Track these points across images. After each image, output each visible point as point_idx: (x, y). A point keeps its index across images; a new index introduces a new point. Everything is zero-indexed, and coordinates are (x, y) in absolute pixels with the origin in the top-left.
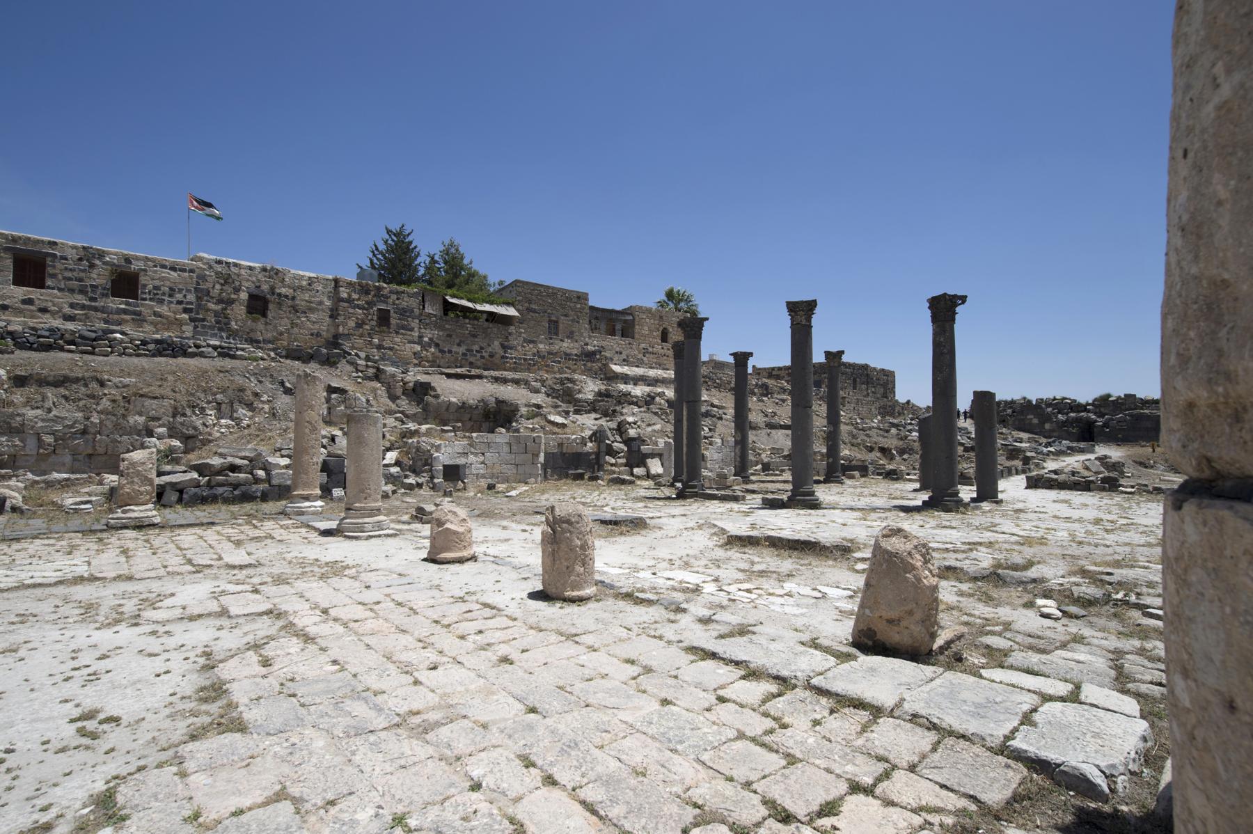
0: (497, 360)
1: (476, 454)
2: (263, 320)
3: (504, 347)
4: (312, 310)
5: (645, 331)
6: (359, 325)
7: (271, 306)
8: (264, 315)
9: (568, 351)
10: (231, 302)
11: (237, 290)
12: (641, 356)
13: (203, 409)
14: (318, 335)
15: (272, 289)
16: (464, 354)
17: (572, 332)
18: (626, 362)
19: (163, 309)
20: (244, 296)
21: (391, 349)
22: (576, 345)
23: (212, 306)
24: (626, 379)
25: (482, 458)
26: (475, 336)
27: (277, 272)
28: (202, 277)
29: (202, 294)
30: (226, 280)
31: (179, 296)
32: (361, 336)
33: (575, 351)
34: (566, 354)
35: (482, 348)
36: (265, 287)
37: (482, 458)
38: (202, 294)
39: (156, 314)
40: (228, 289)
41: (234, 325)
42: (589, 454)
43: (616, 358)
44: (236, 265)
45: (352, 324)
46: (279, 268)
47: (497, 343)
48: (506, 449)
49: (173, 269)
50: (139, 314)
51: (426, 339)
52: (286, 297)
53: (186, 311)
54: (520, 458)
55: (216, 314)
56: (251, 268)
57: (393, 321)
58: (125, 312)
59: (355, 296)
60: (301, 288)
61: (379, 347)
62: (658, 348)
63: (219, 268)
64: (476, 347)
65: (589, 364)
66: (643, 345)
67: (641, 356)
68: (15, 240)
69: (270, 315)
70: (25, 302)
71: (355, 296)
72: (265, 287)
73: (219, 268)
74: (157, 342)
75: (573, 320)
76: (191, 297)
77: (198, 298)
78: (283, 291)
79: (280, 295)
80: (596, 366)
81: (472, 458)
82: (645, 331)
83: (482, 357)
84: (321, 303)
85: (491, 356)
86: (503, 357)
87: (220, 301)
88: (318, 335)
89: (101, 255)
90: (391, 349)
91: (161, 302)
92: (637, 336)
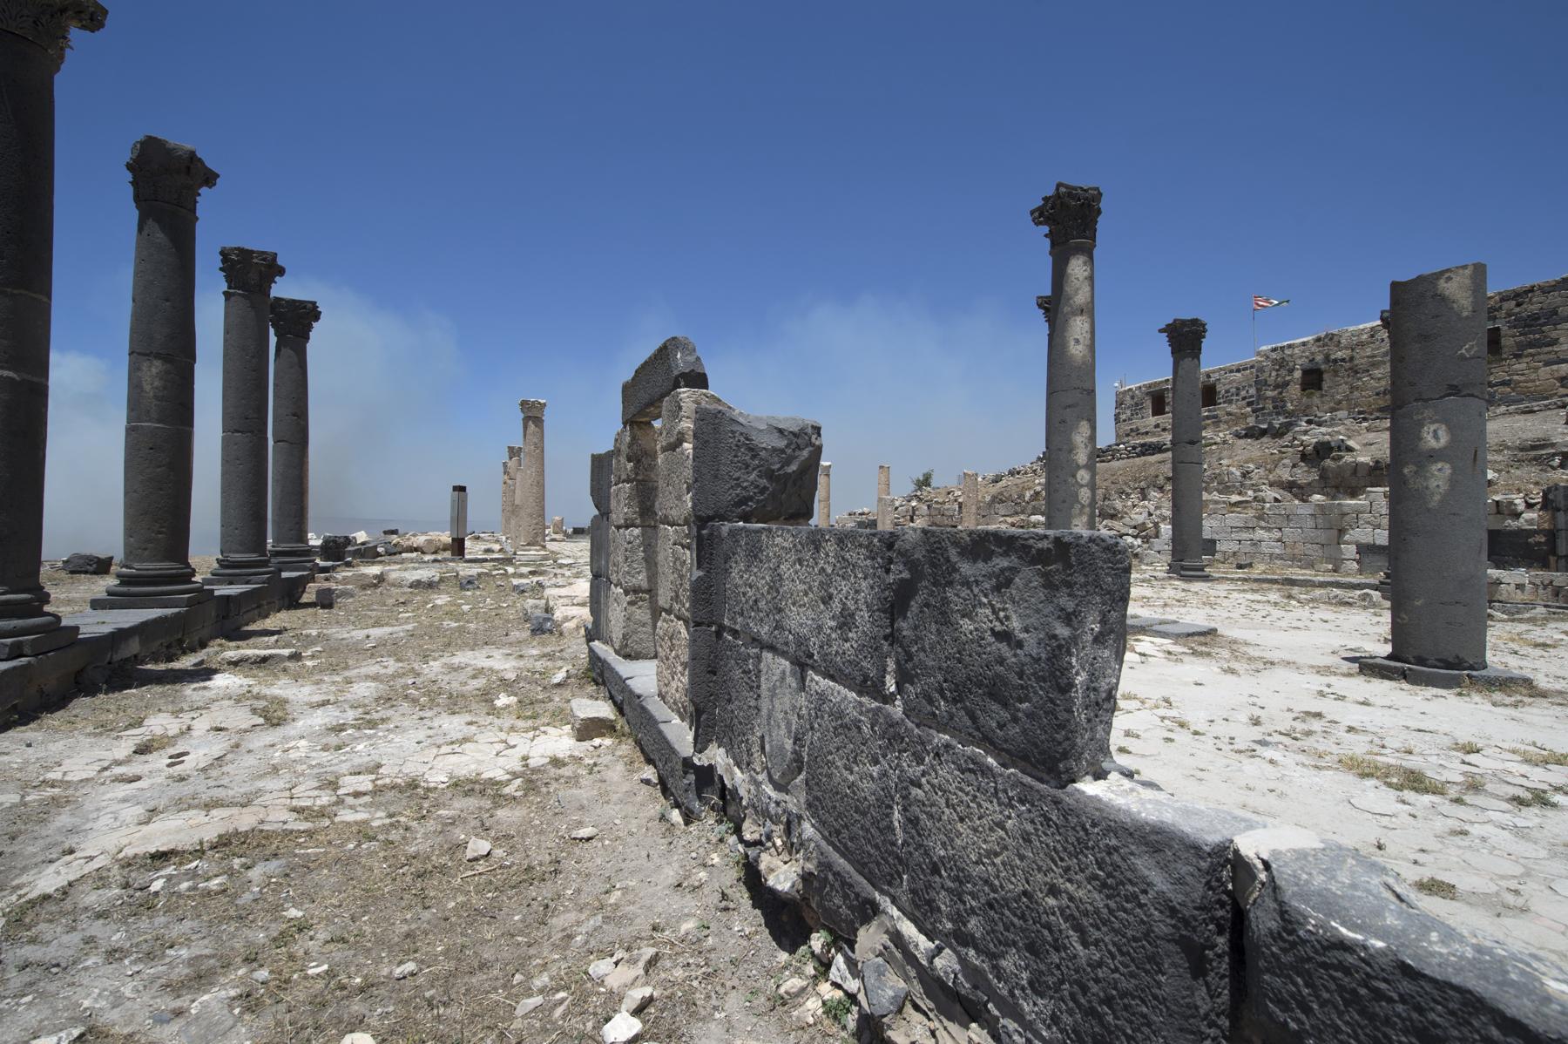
1: (1269, 529)
2: (1318, 393)
7: (1325, 376)
8: (1320, 388)
10: (1287, 384)
11: (1291, 371)
13: (1128, 495)
15: (1327, 357)
19: (1233, 408)
20: (1298, 374)
21: (1503, 383)
27: (1331, 337)
28: (1261, 370)
31: (1243, 393)
36: (1319, 358)
39: (1229, 414)
40: (1283, 372)
41: (1290, 406)
42: (1520, 532)
44: (1290, 346)
46: (1335, 331)
48: (1310, 523)
49: (1238, 371)
50: (1215, 417)
52: (1343, 360)
53: (1249, 404)
54: (1322, 536)
55: (1274, 399)
56: (1304, 344)
60: (1362, 344)
63: (1274, 356)
68: (1150, 386)
69: (1325, 386)
70: (1157, 426)
72: (1319, 358)
73: (1274, 356)
74: (1142, 445)
76: (1252, 391)
77: (1258, 390)
78: (1339, 354)
79: (1335, 361)
81: (1260, 534)
87: (1277, 387)
90: (1503, 383)
91: (1230, 402)
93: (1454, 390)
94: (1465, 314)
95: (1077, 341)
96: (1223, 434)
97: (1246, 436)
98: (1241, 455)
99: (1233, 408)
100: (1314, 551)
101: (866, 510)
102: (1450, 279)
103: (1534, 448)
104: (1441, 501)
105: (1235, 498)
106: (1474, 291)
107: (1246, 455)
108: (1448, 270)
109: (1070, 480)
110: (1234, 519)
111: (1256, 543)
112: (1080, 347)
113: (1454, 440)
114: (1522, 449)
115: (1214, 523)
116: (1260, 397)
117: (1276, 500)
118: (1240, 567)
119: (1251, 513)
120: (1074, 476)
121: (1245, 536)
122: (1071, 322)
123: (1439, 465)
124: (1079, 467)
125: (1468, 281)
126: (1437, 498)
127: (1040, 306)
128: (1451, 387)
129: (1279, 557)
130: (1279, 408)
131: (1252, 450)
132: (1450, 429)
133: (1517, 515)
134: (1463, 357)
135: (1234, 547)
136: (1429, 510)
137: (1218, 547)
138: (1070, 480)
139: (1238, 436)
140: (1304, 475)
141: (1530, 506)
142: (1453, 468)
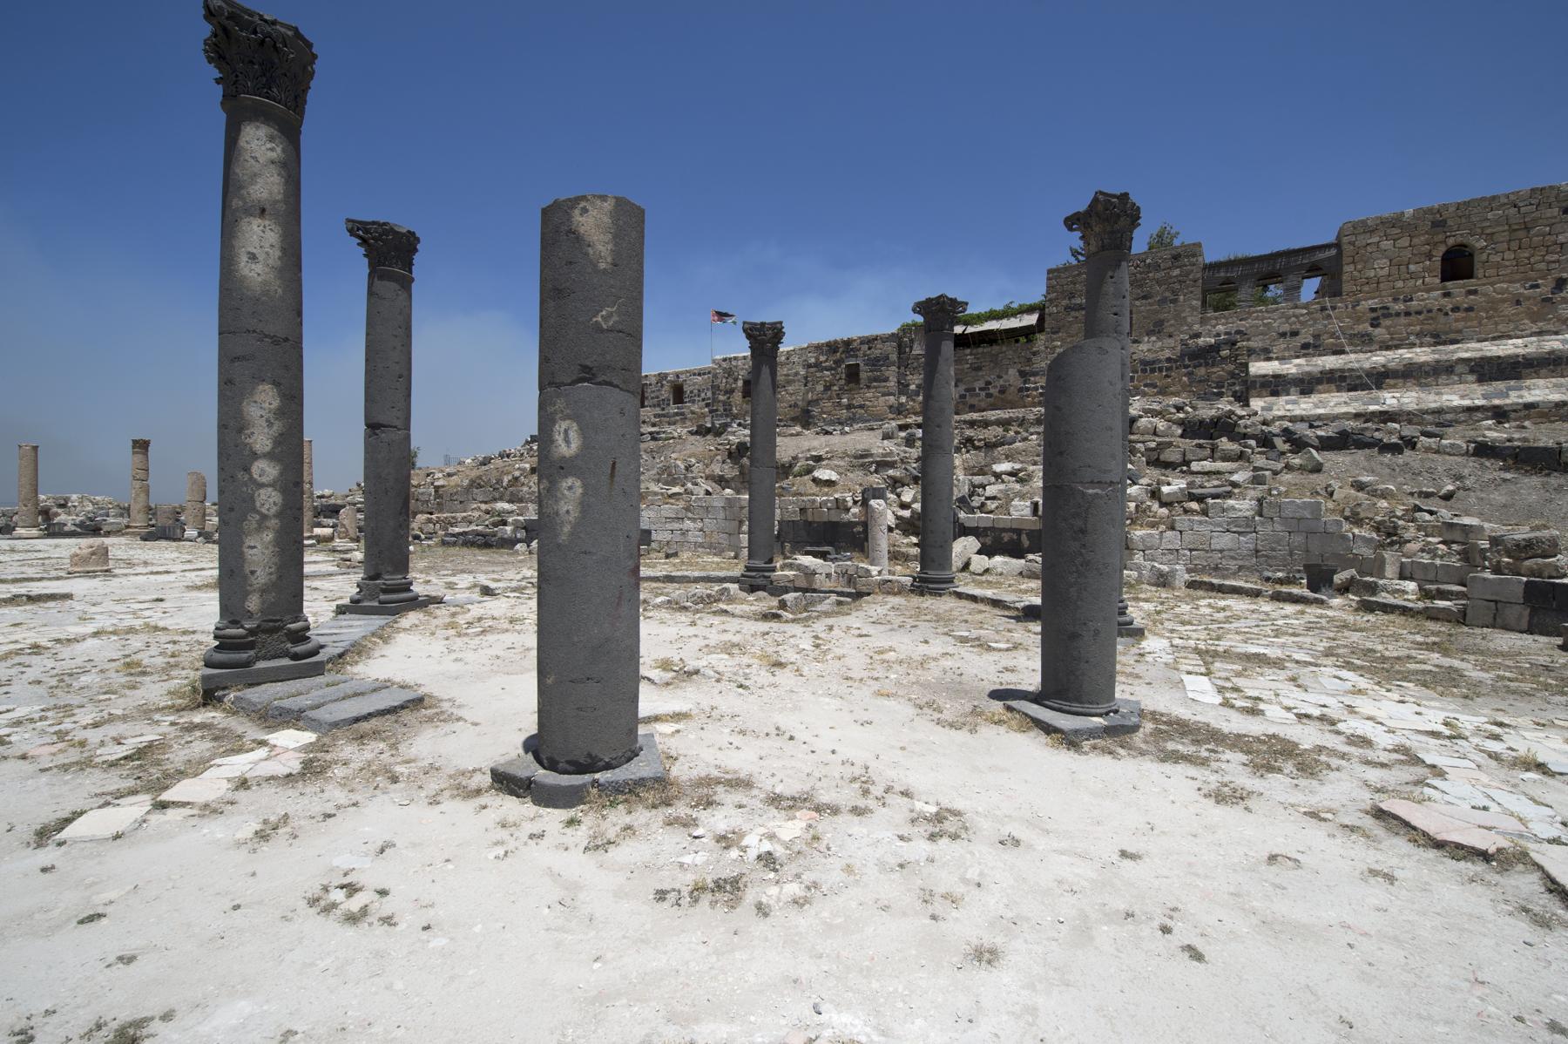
0: (1012, 394)
1: (693, 520)
3: (1022, 374)
4: (789, 382)
5: (1381, 267)
6: (827, 388)
9: (1150, 356)
10: (732, 391)
11: (736, 380)
12: (1365, 327)
14: (796, 405)
16: (962, 396)
17: (1160, 323)
18: (1307, 349)
19: (695, 408)
20: (740, 383)
21: (861, 407)
22: (1171, 342)
23: (721, 398)
24: (1275, 386)
25: (700, 525)
26: (979, 369)
28: (715, 376)
29: (715, 388)
30: (729, 373)
32: (830, 398)
33: (1167, 354)
34: (1144, 363)
35: (988, 383)
37: (700, 525)
38: (715, 388)
41: (735, 411)
42: (851, 524)
43: (1281, 345)
44: (735, 358)
45: (820, 388)
47: (1013, 372)
51: (913, 387)
55: (724, 403)
57: (863, 375)
58: (677, 414)
59: (822, 358)
61: (849, 407)
62: (1434, 299)
63: (724, 365)
64: (979, 384)
65: (1202, 371)
66: (1371, 303)
67: (1365, 327)
71: (822, 358)
73: (724, 365)
75: (1163, 301)
76: (709, 394)
80: (1219, 372)
81: (688, 524)
82: (1381, 267)
83: (989, 395)
84: (797, 374)
85: (1002, 391)
86: (1021, 390)
87: (726, 392)
88: (796, 405)
89: (666, 375)
90: (861, 407)
92: (1346, 287)
93: (587, 374)
94: (602, 266)
95: (253, 257)
96: (679, 430)
97: (696, 433)
98: (690, 449)
99: (695, 408)
100: (723, 539)
101: (327, 492)
102: (584, 210)
103: (862, 457)
104: (571, 534)
105: (676, 489)
106: (615, 236)
107: (692, 449)
108: (584, 198)
109: (241, 476)
110: (668, 510)
111: (684, 533)
112: (258, 268)
113: (586, 446)
114: (855, 457)
115: (652, 514)
116: (715, 400)
117: (708, 493)
118: (667, 556)
119: (681, 504)
120: (247, 470)
121: (676, 526)
122: (244, 224)
123: (570, 481)
124: (255, 456)
125: (607, 220)
126: (567, 529)
127: (352, 232)
128: (585, 368)
129: (701, 545)
130: (728, 412)
131: (700, 445)
132: (583, 431)
133: (848, 510)
134: (598, 328)
135: (667, 536)
136: (559, 545)
137: (654, 536)
138: (241, 476)
139: (691, 433)
140: (729, 471)
141: (855, 502)
142: (585, 486)
